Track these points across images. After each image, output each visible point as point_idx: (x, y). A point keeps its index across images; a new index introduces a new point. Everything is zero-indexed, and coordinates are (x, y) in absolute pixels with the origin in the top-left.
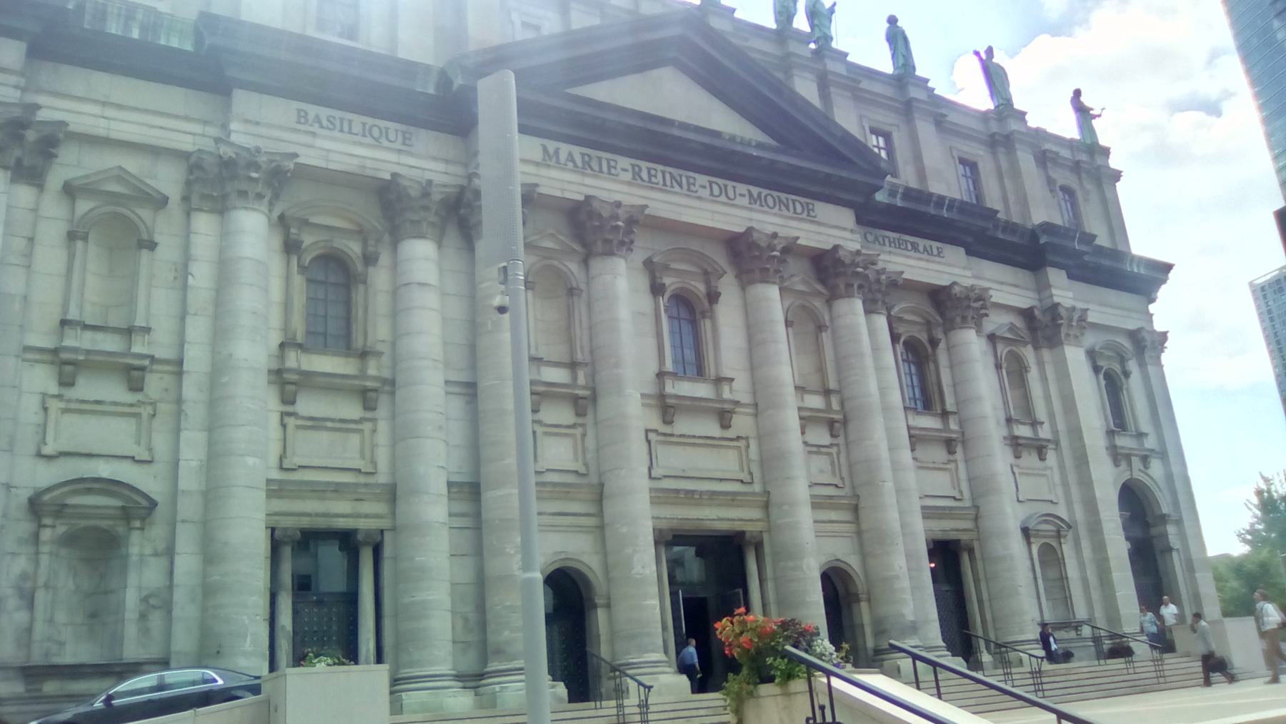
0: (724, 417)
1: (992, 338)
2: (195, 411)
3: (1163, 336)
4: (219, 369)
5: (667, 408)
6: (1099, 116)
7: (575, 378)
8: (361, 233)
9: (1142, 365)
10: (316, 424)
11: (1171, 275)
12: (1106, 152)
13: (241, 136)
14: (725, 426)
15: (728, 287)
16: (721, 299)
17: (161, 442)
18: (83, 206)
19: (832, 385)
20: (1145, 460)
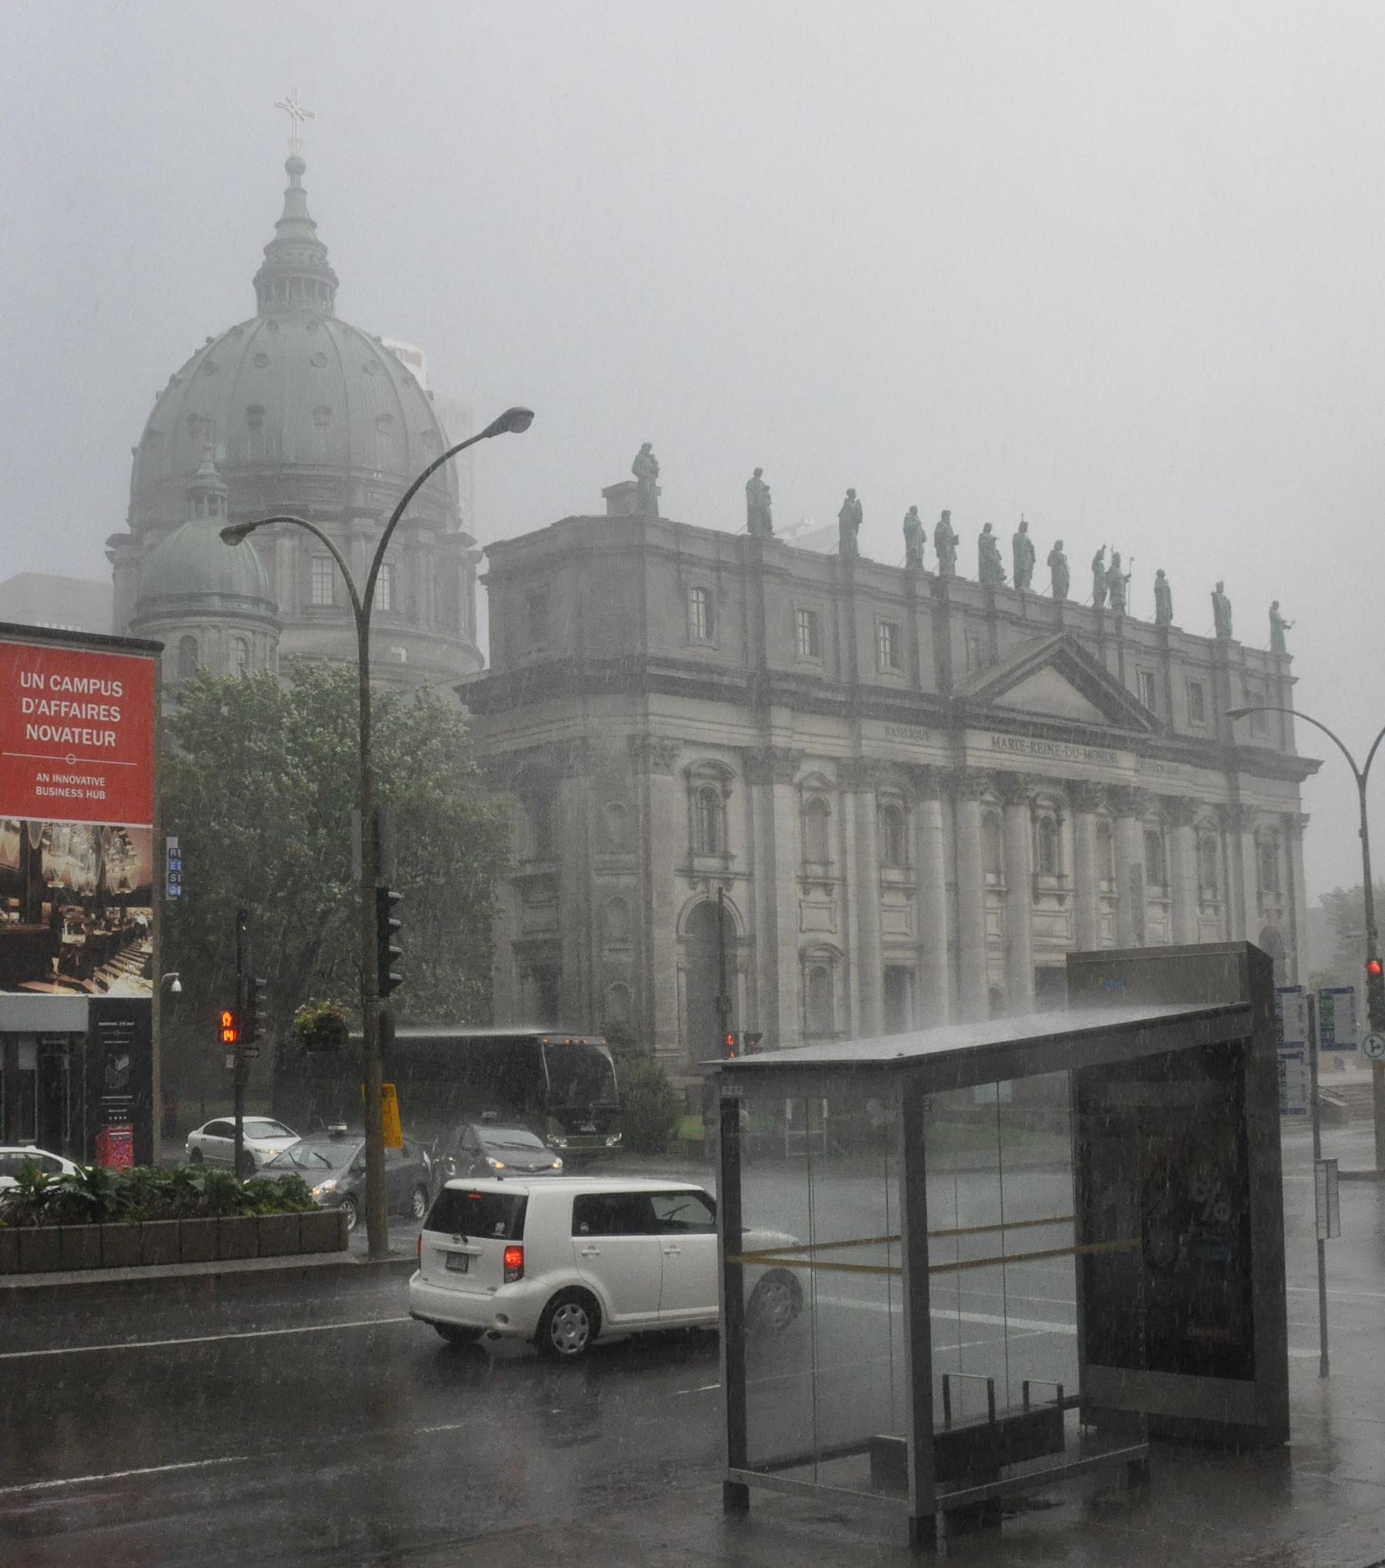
0: (1061, 899)
1: (1196, 829)
2: (853, 907)
3: (1306, 817)
4: (861, 885)
5: (1037, 895)
6: (1289, 628)
7: (999, 880)
8: (904, 798)
9: (1288, 839)
10: (891, 908)
11: (1320, 769)
12: (1289, 658)
13: (867, 749)
14: (1061, 904)
15: (1066, 814)
16: (1064, 823)
17: (838, 921)
18: (806, 795)
19: (1114, 876)
20: (1279, 912)
